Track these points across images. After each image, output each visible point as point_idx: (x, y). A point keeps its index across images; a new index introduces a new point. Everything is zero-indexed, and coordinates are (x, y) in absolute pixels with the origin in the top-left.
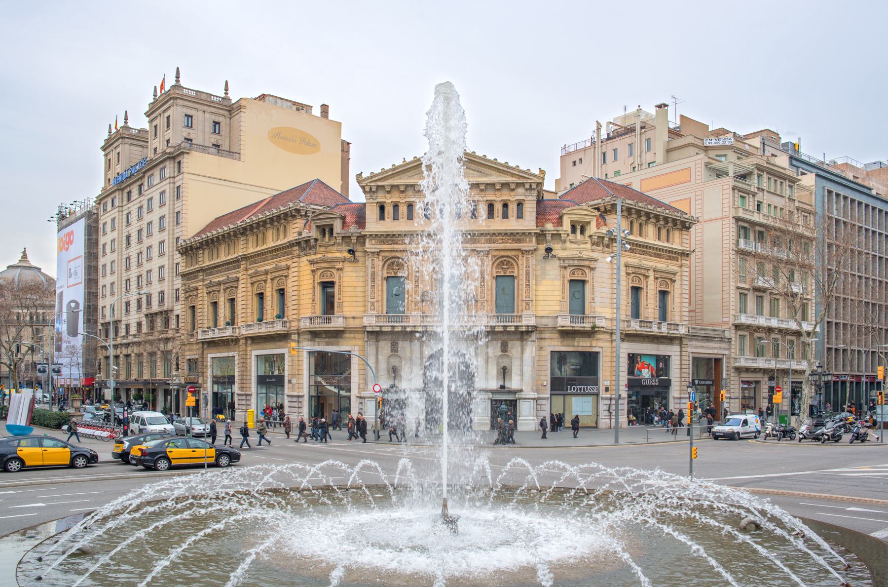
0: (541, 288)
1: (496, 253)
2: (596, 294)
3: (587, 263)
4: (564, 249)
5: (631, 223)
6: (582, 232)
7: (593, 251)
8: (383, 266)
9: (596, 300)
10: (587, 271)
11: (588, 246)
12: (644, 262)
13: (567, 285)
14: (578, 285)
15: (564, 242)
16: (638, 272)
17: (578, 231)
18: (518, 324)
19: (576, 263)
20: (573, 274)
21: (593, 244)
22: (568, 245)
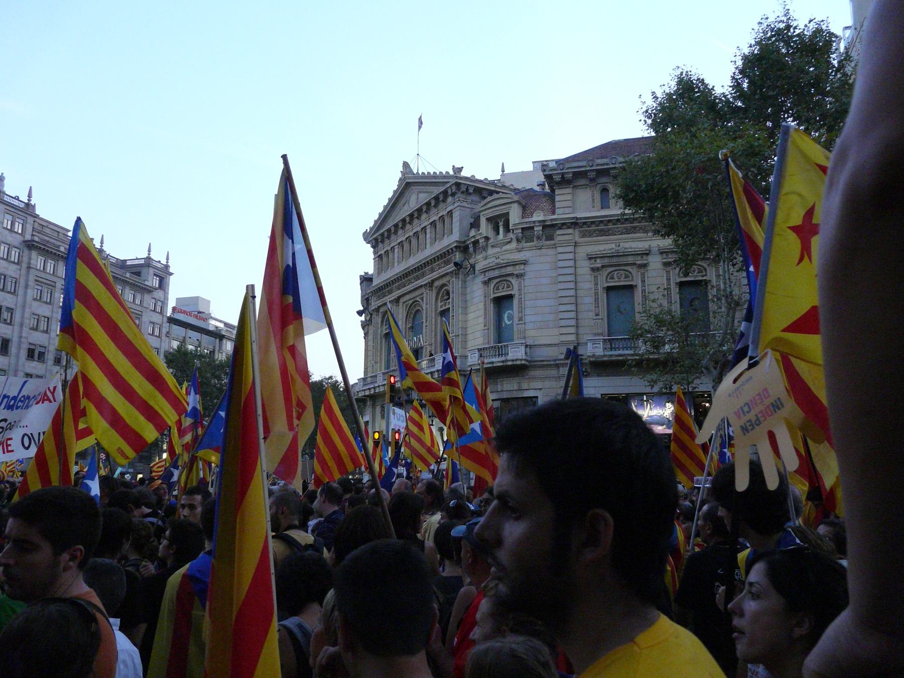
0: (471, 316)
1: (437, 284)
2: (528, 311)
3: (509, 270)
4: (486, 258)
5: (605, 191)
6: (507, 229)
7: (520, 250)
8: (382, 322)
9: (528, 319)
10: (513, 281)
11: (514, 245)
12: (627, 245)
13: (491, 307)
14: (501, 302)
15: (485, 249)
16: (615, 262)
17: (501, 230)
18: (433, 370)
19: (496, 273)
20: (498, 289)
21: (518, 240)
22: (491, 251)
